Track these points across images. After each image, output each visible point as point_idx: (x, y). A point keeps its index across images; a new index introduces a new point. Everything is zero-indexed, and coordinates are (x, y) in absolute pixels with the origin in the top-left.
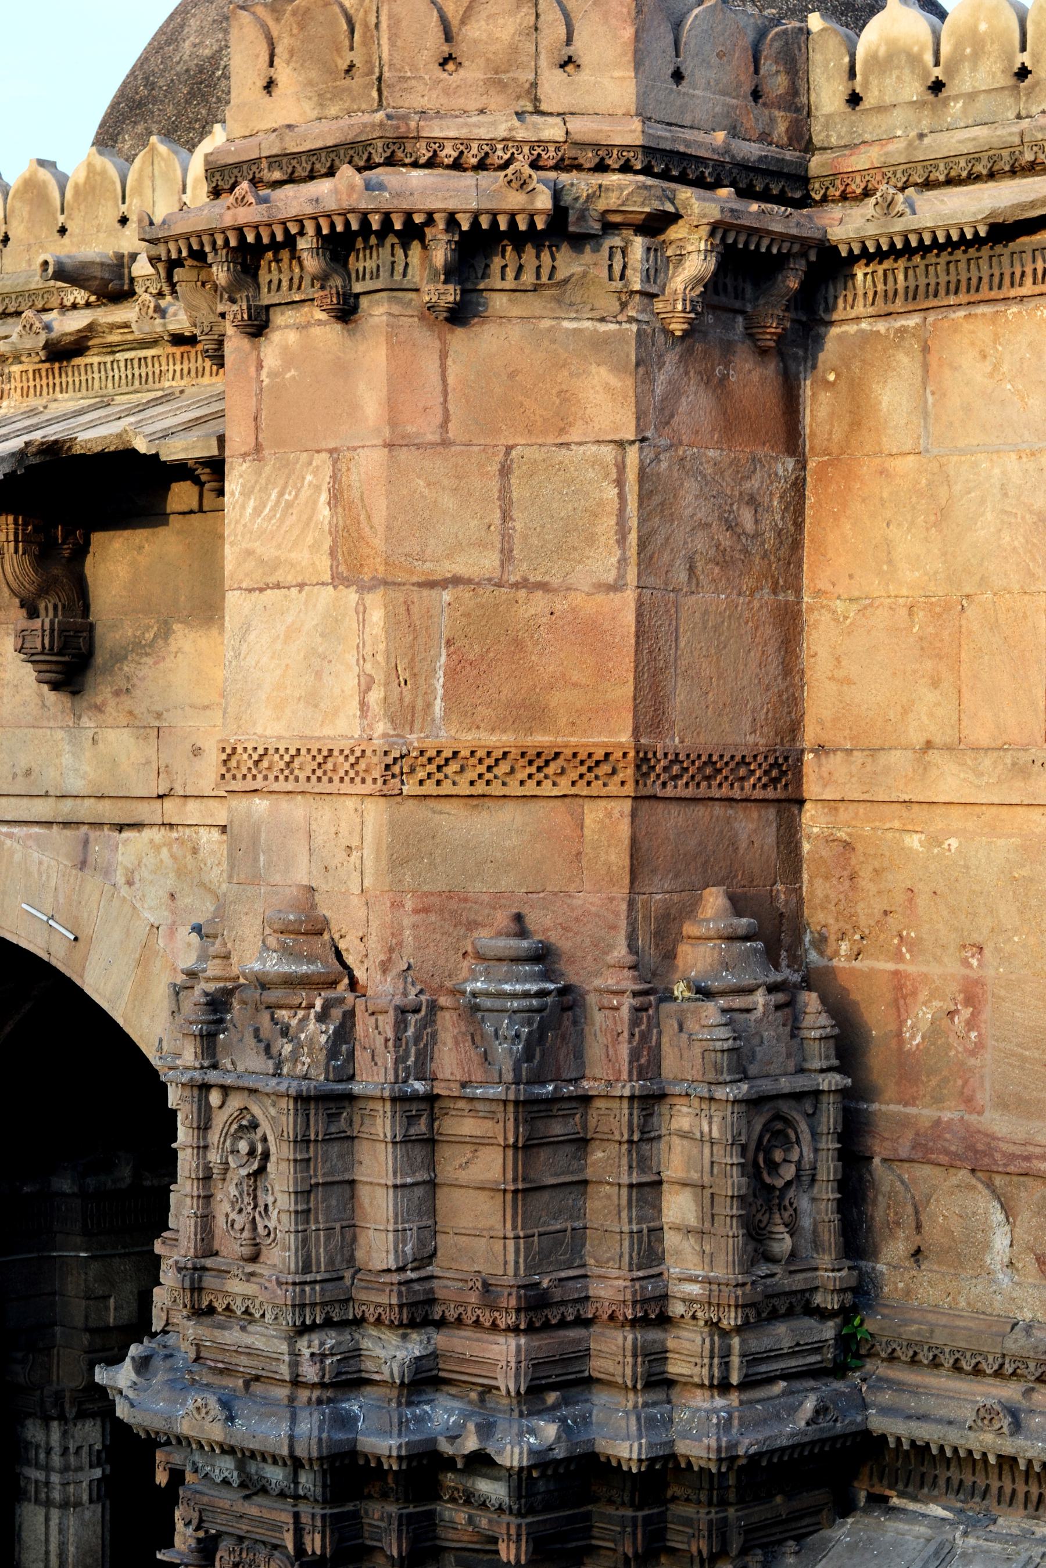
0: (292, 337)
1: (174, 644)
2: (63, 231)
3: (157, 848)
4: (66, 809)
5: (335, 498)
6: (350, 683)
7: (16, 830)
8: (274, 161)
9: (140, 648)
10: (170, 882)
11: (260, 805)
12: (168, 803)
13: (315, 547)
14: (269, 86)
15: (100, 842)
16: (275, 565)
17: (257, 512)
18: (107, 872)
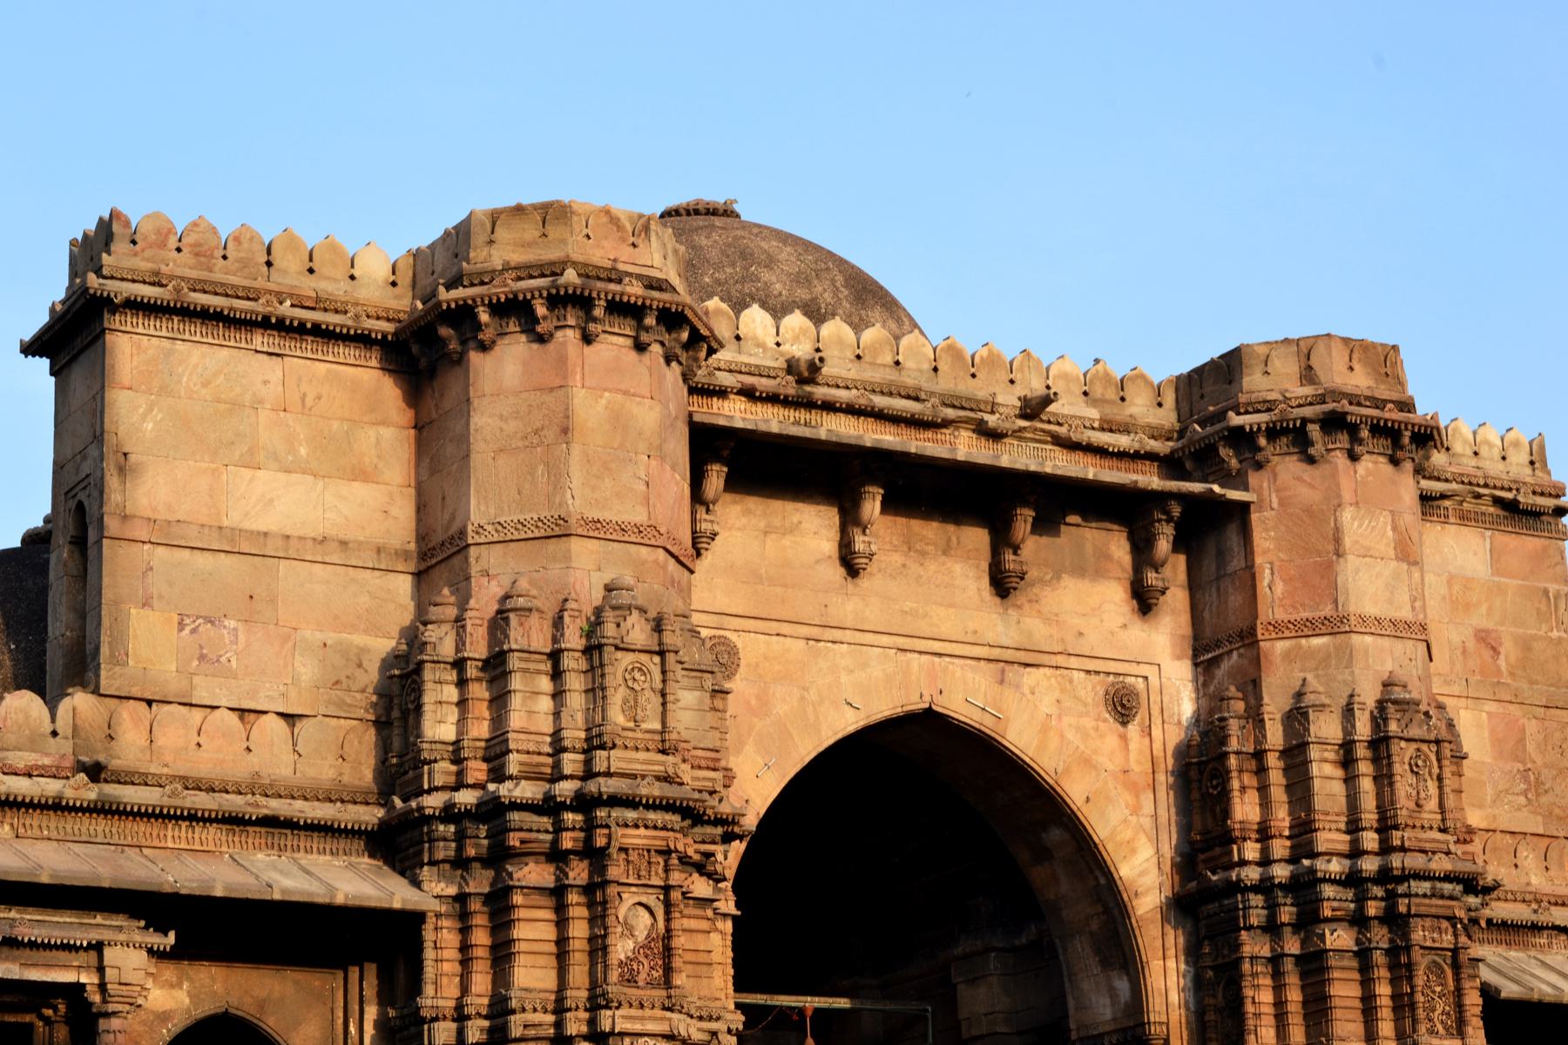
0: (1370, 465)
1: (1063, 583)
2: (973, 376)
3: (1049, 678)
4: (996, 653)
5: (1394, 529)
6: (1406, 597)
7: (956, 661)
8: (1367, 398)
9: (1042, 581)
10: (1057, 694)
11: (1368, 639)
12: (1059, 657)
13: (1387, 545)
14: (1351, 369)
15: (1012, 673)
16: (1369, 549)
17: (1360, 526)
18: (1018, 686)
